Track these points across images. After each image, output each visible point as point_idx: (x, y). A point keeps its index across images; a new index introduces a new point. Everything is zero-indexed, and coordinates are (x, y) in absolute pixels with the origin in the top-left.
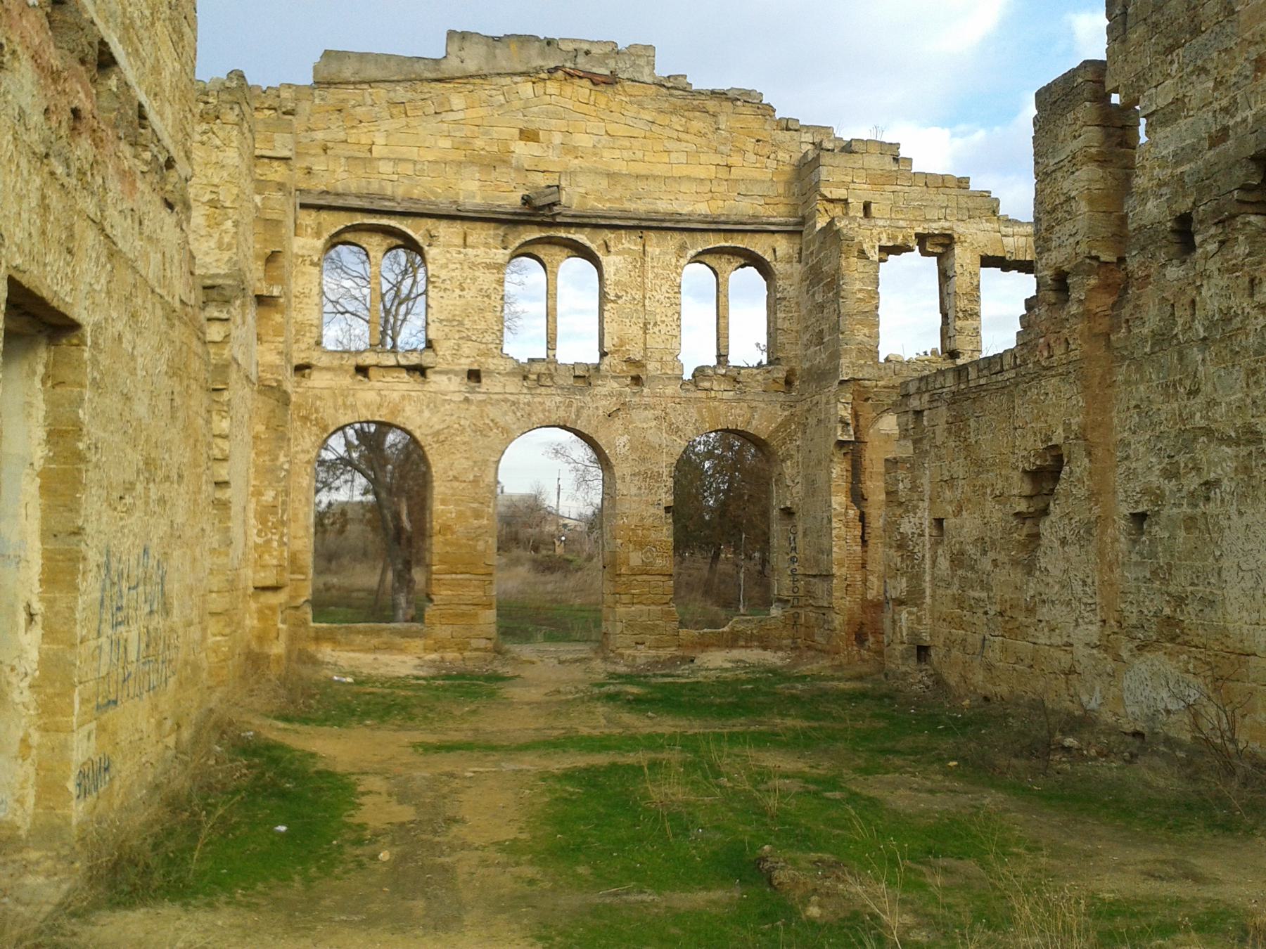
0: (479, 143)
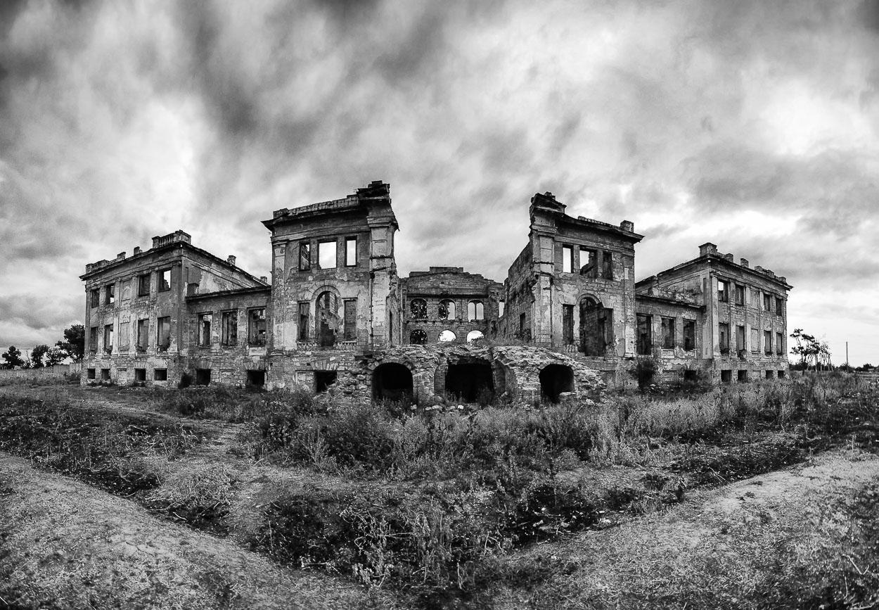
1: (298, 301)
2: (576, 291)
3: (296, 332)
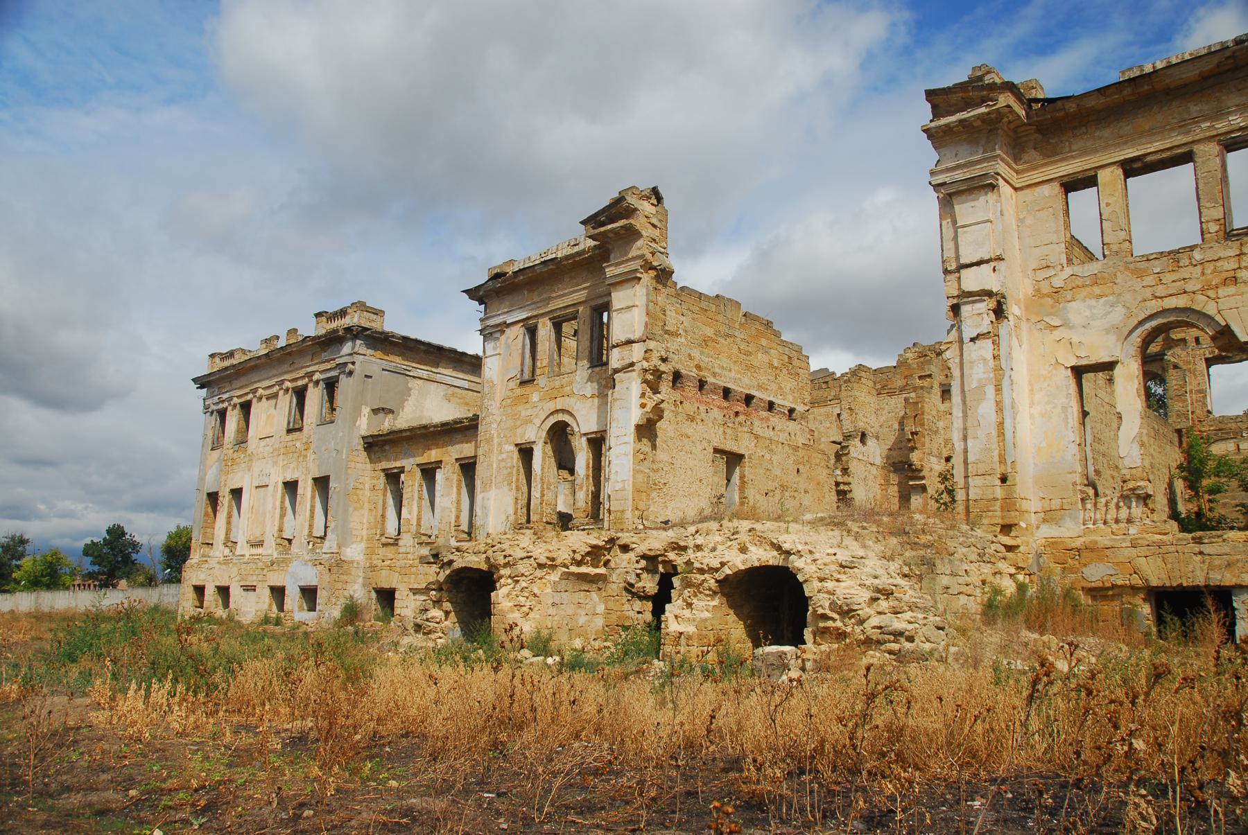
1: (517, 445)
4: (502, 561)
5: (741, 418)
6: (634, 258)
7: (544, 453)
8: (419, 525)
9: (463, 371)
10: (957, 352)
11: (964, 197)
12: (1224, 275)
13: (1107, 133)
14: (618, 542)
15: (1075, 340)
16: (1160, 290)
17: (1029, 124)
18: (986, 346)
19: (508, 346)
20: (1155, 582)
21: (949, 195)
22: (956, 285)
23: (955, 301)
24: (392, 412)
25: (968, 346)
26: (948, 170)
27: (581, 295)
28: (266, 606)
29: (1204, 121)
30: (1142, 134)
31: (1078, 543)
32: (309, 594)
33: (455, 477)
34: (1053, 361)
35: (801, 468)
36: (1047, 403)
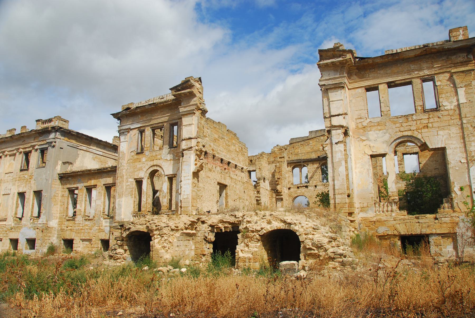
0: (314, 148)
2: (387, 137)
3: (132, 206)
4: (155, 228)
5: (227, 171)
6: (193, 105)
7: (148, 183)
8: (85, 212)
9: (100, 148)
10: (330, 148)
11: (332, 90)
12: (424, 125)
13: (382, 72)
14: (201, 220)
15: (372, 145)
16: (402, 129)
17: (355, 66)
18: (341, 146)
19: (131, 138)
20: (402, 233)
21: (326, 90)
22: (329, 123)
23: (329, 129)
24: (71, 163)
25: (334, 146)
26: (326, 80)
27: (166, 119)
28: (8, 248)
29: (416, 71)
30: (395, 73)
31: (374, 219)
32: (31, 243)
33: (103, 192)
34: (364, 153)
35: (245, 190)
36: (362, 168)
